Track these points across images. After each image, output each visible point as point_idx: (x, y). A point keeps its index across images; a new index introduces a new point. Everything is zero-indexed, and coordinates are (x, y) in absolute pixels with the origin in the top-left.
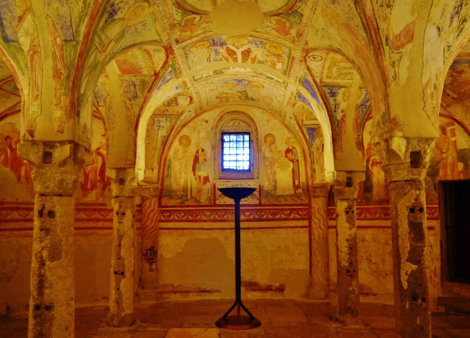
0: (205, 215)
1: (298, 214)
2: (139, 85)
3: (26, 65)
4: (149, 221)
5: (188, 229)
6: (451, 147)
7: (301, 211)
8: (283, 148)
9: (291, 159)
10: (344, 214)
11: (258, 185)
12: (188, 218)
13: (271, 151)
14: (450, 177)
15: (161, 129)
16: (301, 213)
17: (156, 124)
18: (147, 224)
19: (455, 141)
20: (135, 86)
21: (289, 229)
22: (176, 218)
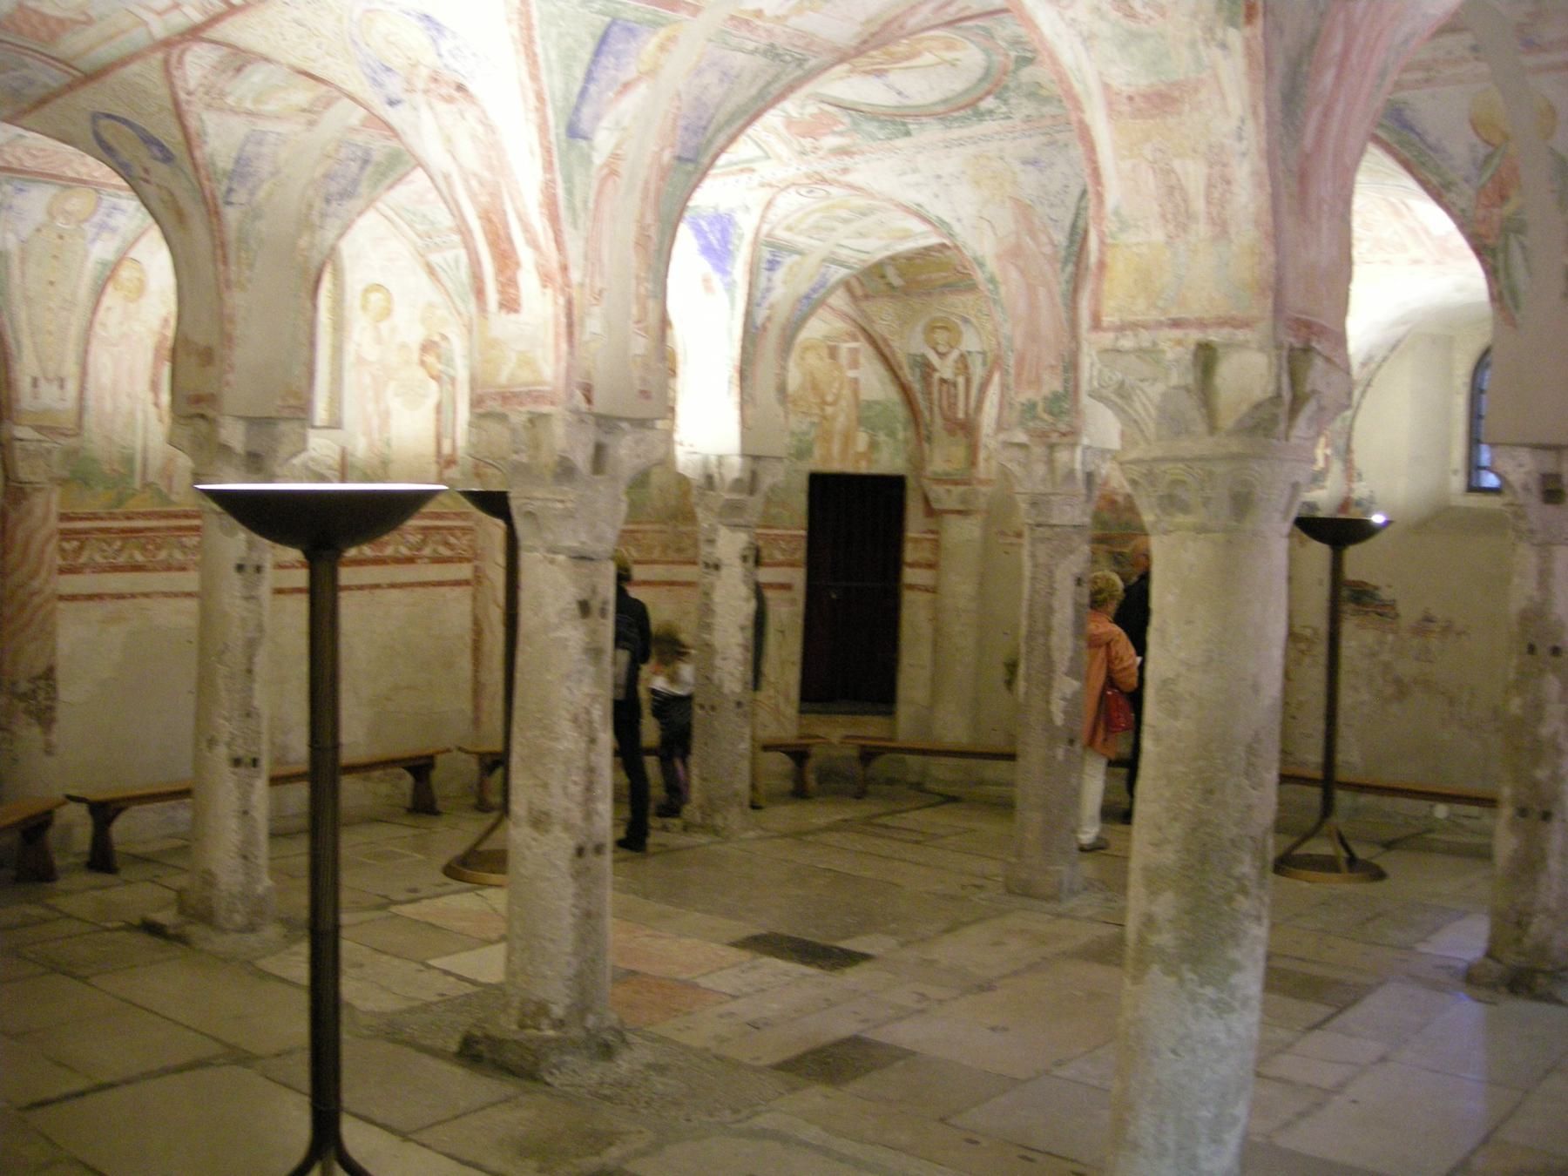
0: (183, 547)
1: (447, 544)
2: (378, 164)
3: (585, 202)
4: (44, 574)
5: (133, 596)
6: (847, 392)
7: (453, 535)
8: (415, 335)
9: (435, 373)
10: (738, 562)
11: (337, 449)
12: (131, 556)
13: (379, 341)
14: (837, 466)
15: (105, 236)
16: (452, 540)
17: (96, 219)
18: (36, 584)
19: (856, 381)
20: (366, 162)
21: (420, 590)
22: (99, 559)
